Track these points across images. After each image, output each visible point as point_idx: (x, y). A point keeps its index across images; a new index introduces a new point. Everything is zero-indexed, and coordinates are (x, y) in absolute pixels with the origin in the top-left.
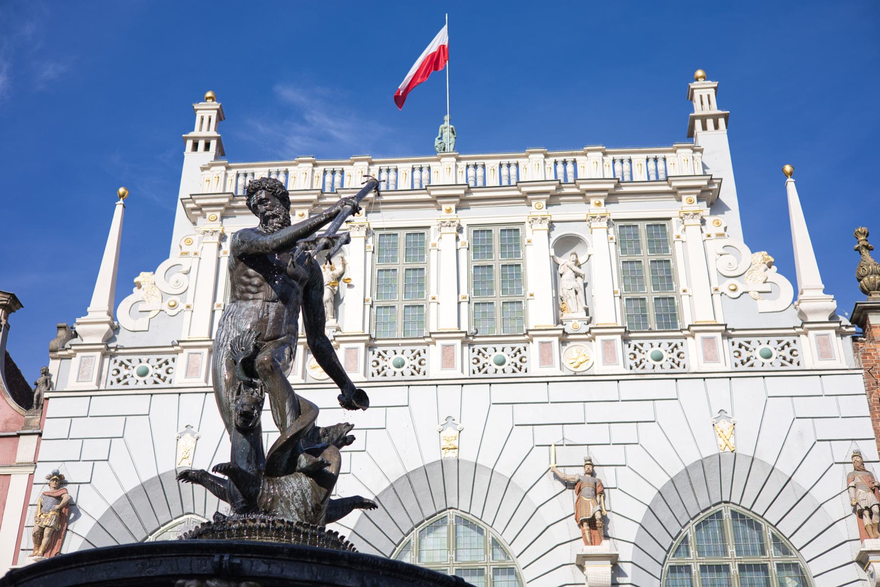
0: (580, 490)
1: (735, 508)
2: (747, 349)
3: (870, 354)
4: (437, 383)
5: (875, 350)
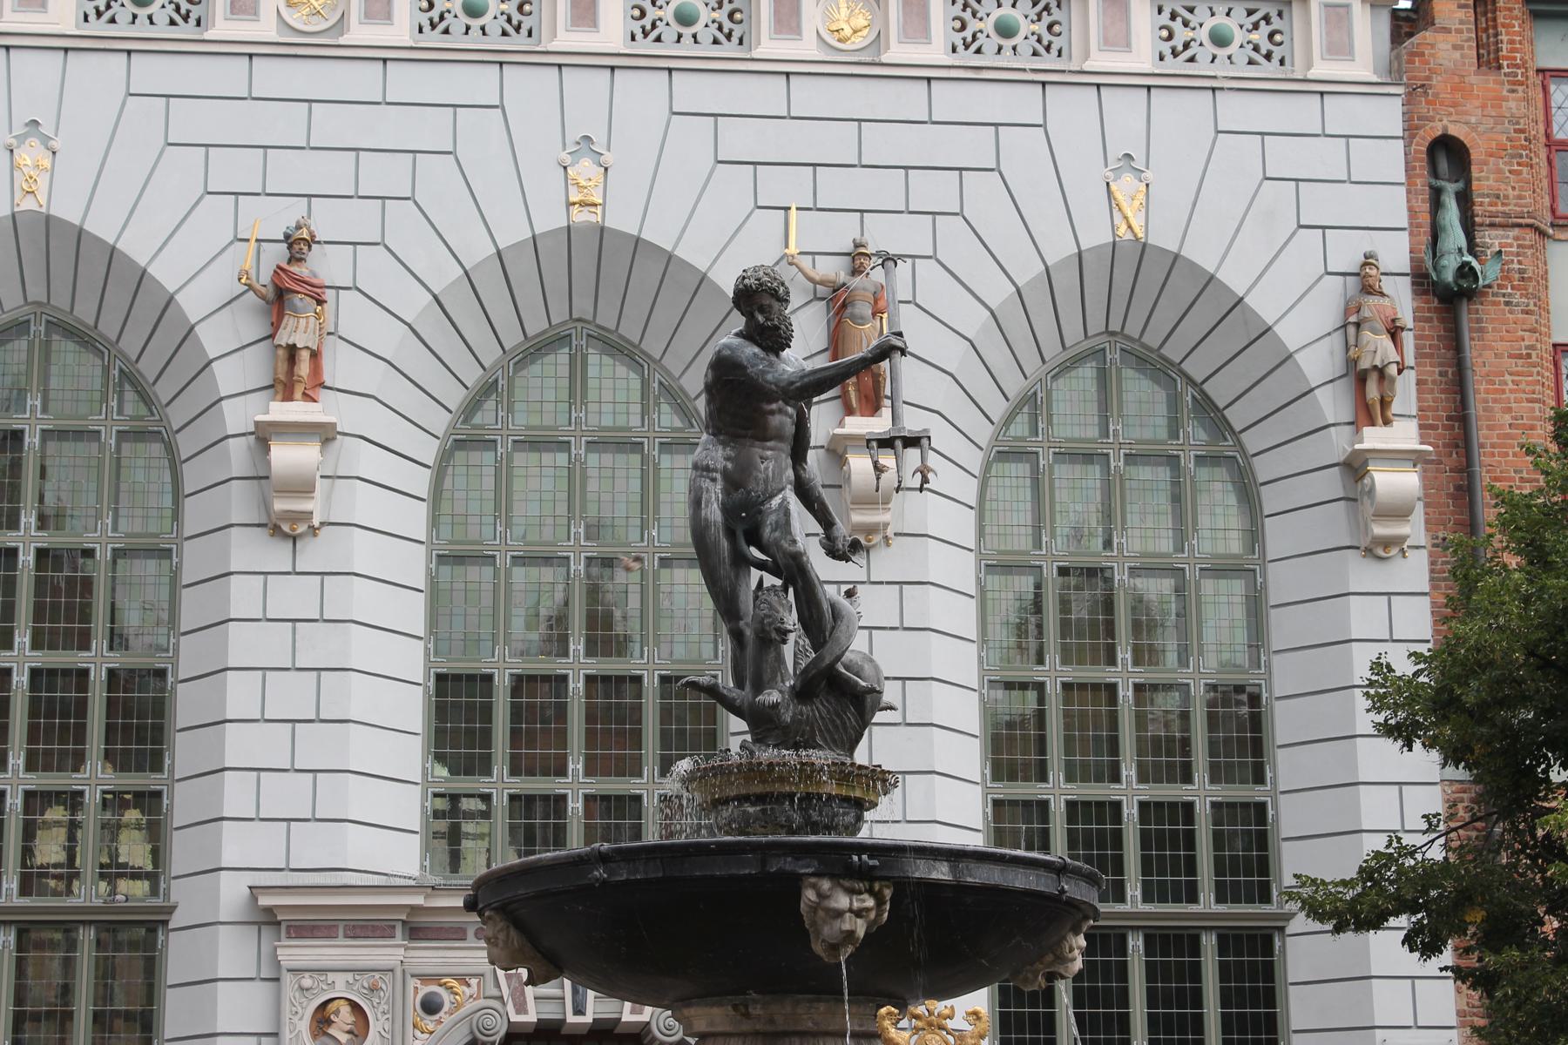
0: (844, 305)
1: (1128, 345)
2: (1186, 24)
3: (1423, 54)
4: (561, 63)
5: (1432, 46)
